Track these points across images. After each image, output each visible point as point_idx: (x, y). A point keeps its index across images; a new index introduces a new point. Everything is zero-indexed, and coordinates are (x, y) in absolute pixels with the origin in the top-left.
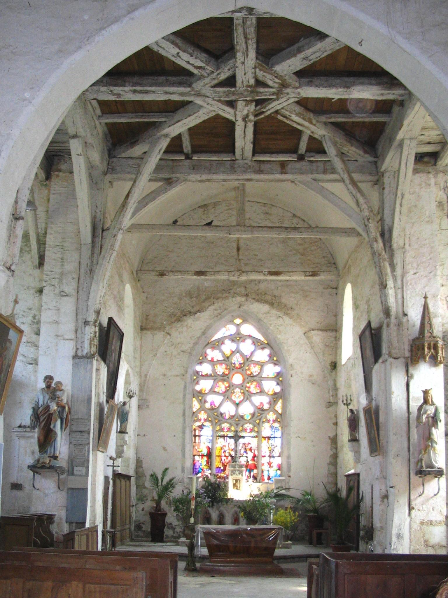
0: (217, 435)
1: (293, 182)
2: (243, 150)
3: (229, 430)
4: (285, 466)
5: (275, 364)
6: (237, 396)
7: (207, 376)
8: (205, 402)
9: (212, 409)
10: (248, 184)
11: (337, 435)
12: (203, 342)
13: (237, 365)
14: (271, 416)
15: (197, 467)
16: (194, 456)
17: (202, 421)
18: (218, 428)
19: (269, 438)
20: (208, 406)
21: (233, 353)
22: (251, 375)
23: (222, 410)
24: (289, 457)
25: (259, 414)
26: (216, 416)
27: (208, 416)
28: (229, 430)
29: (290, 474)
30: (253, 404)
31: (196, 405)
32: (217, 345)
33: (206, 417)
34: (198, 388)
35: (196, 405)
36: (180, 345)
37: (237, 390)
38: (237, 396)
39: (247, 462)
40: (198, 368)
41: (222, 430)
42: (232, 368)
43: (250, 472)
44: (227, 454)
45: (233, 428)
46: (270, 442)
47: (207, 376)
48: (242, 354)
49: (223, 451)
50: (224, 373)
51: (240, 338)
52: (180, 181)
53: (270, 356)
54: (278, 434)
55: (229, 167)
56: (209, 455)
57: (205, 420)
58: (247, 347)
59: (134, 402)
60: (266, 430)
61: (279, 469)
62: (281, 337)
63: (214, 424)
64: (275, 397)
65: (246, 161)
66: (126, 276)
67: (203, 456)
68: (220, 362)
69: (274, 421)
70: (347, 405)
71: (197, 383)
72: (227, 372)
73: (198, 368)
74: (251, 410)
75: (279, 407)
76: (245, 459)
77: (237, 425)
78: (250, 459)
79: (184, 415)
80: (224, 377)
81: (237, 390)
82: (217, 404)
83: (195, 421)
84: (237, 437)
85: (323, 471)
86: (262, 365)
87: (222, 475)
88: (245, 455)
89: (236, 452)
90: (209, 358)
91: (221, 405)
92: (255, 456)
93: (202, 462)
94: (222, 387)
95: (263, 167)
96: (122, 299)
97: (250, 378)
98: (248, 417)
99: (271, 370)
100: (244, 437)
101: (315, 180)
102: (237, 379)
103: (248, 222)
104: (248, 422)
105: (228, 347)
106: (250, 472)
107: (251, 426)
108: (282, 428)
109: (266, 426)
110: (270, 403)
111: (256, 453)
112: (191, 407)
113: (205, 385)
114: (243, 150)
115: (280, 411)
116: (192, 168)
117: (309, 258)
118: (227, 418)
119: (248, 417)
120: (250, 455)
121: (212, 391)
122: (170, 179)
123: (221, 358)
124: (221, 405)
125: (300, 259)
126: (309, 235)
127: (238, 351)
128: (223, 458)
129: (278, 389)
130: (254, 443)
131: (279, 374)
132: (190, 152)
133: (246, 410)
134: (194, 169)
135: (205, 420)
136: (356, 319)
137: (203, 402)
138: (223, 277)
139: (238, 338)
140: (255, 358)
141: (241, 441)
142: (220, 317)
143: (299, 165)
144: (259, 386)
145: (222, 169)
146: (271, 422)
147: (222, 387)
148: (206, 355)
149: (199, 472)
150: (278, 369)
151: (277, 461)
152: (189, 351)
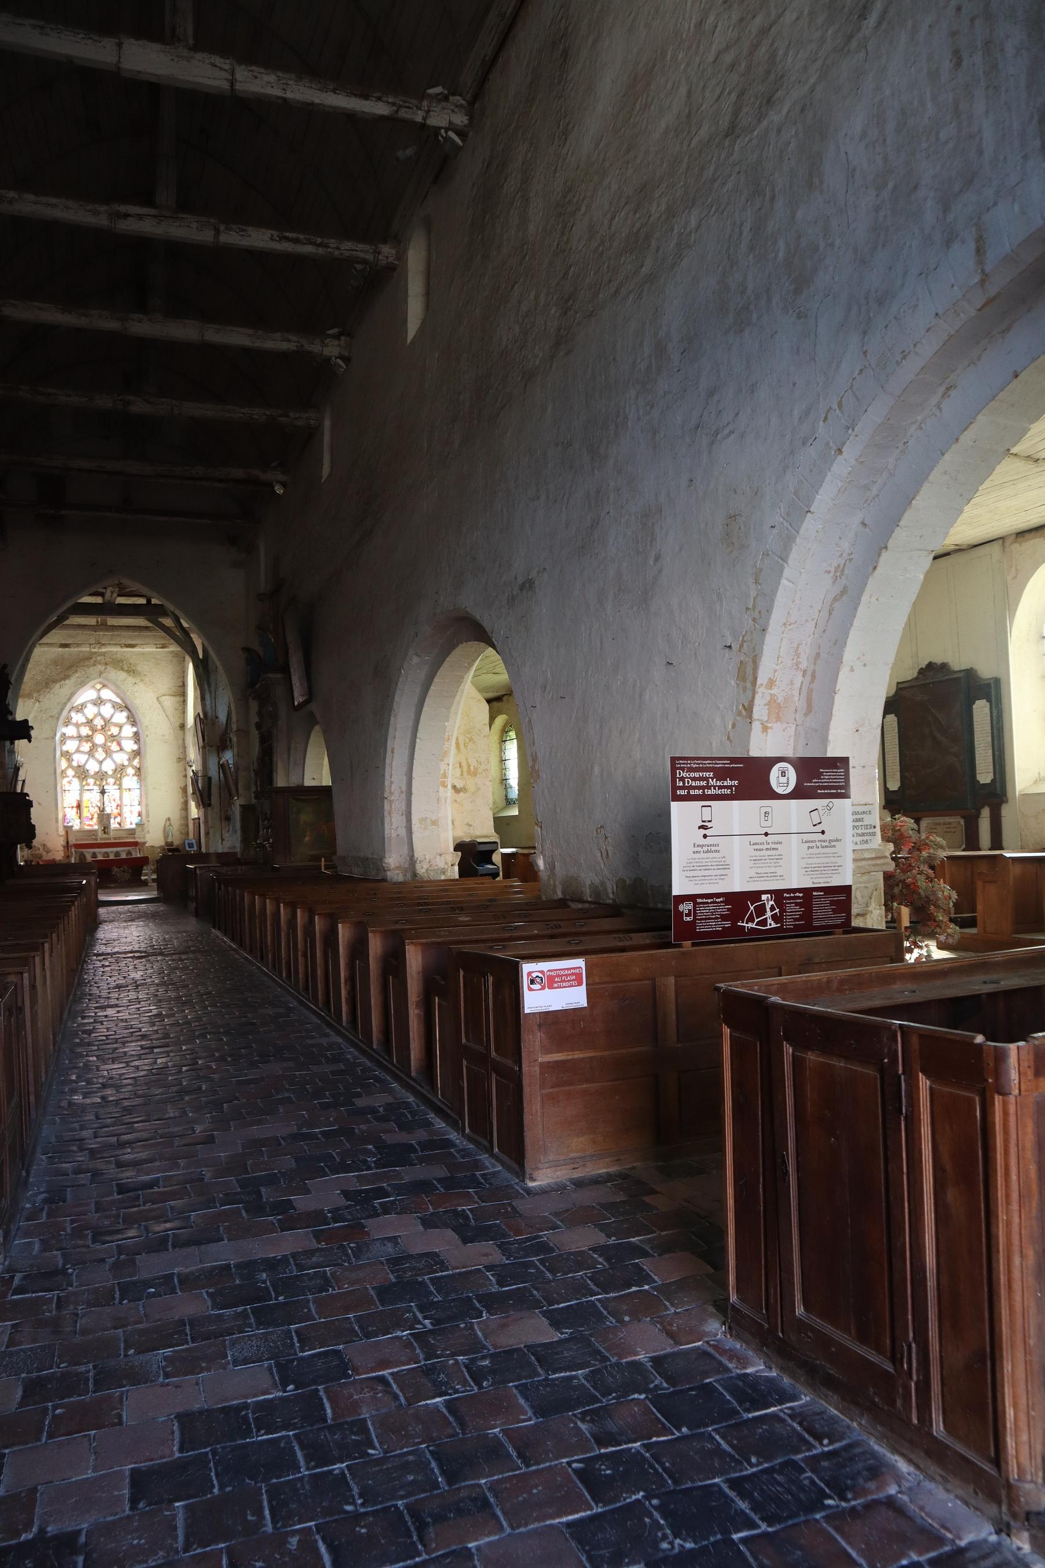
4: (144, 813)
6: (100, 754)
12: (68, 708)
14: (131, 771)
20: (75, 764)
21: (95, 716)
22: (112, 736)
23: (87, 767)
24: (147, 806)
25: (120, 770)
26: (82, 773)
30: (114, 761)
31: (64, 764)
32: (80, 709)
34: (65, 748)
35: (64, 764)
37: (100, 750)
38: (100, 754)
40: (64, 730)
41: (88, 784)
47: (72, 737)
48: (103, 718)
62: (137, 702)
72: (90, 733)
75: (136, 763)
80: (89, 738)
81: (100, 750)
87: (91, 823)
90: (74, 721)
94: (86, 747)
98: (110, 773)
105: (91, 711)
113: (71, 746)
119: (110, 773)
120: (114, 805)
121: (78, 751)
129: (135, 747)
133: (108, 767)
138: (85, 649)
139: (99, 702)
140: (114, 720)
144: (119, 744)
147: (86, 747)
150: (135, 729)
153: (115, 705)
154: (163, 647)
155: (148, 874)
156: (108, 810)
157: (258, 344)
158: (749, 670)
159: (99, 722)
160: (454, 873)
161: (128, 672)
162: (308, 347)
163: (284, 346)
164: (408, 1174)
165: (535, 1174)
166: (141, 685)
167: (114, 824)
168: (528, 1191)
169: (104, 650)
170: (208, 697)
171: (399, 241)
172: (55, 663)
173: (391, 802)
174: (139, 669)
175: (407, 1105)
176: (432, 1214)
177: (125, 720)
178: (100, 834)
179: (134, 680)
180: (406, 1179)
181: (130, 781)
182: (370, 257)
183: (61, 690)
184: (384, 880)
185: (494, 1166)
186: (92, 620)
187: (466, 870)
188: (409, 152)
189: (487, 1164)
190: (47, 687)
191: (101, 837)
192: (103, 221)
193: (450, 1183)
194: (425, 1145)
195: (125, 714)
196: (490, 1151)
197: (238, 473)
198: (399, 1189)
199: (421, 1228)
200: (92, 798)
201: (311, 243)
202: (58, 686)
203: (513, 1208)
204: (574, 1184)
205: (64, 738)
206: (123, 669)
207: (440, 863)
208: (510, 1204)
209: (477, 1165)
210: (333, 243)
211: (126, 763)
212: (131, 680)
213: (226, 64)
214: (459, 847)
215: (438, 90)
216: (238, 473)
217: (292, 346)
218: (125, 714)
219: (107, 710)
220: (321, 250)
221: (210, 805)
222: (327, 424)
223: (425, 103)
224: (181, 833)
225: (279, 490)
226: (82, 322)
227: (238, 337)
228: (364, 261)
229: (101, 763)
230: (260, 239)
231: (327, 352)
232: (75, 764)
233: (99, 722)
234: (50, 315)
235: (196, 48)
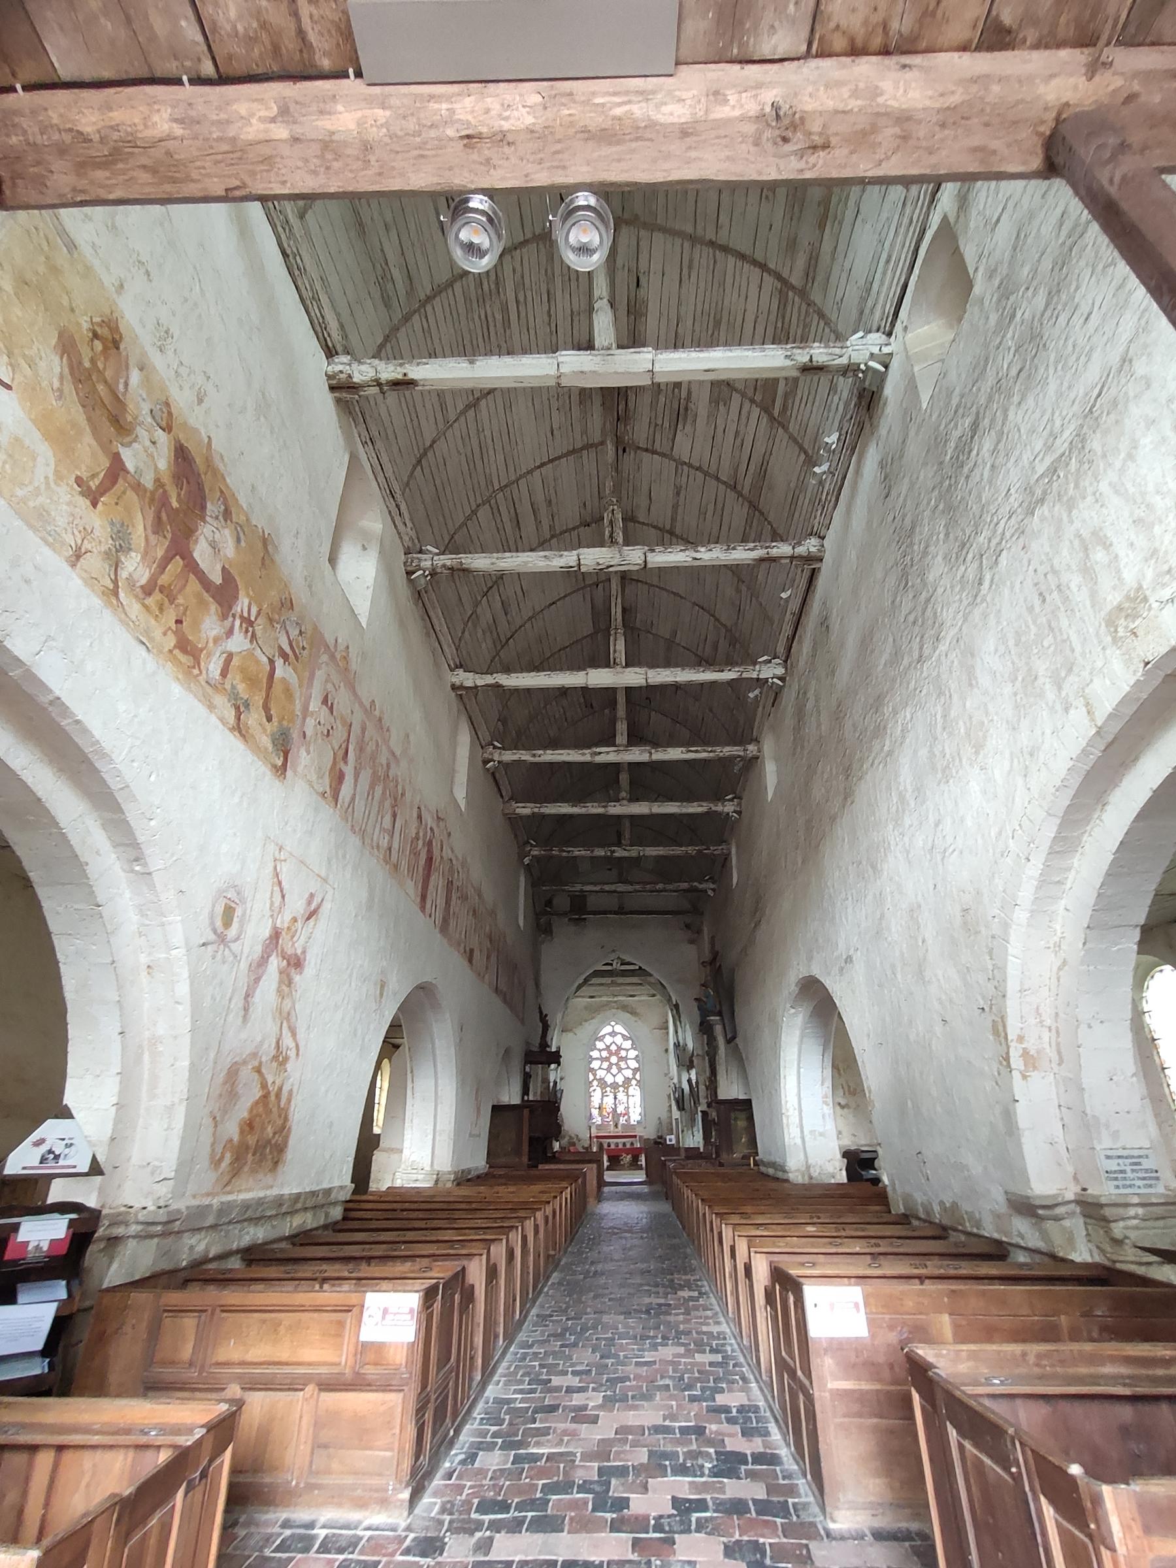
6: (614, 1070)
14: (634, 1082)
25: (627, 1081)
26: (603, 1083)
32: (601, 1039)
35: (591, 1077)
38: (614, 1070)
42: (611, 1054)
60: (631, 1091)
64: (635, 1070)
75: (638, 1077)
86: (627, 1050)
93: (595, 1112)
94: (605, 1065)
99: (633, 1054)
102: (614, 1059)
105: (608, 1040)
133: (620, 1079)
137: (595, 1075)
147: (605, 1065)
150: (636, 1053)
151: (639, 1110)
153: (623, 1035)
157: (684, 811)
158: (1001, 1028)
159: (614, 1048)
160: (843, 1177)
162: (714, 808)
163: (700, 810)
164: (734, 1489)
165: (836, 1514)
167: (622, 1121)
168: (828, 1534)
171: (757, 741)
173: (788, 1117)
175: (756, 1409)
176: (737, 1541)
180: (729, 1495)
181: (635, 1091)
182: (742, 753)
183: (589, 1027)
184: (787, 1181)
185: (806, 1495)
186: (608, 980)
187: (852, 1174)
188: (757, 692)
189: (802, 1491)
191: (612, 1131)
192: (588, 758)
193: (764, 1507)
194: (759, 1458)
196: (805, 1476)
197: (685, 885)
198: (720, 1506)
199: (722, 1557)
200: (609, 1101)
201: (705, 751)
203: (808, 1551)
204: (873, 1535)
205: (592, 1059)
207: (830, 1169)
208: (807, 1546)
209: (792, 1490)
210: (718, 749)
212: (634, 1019)
213: (642, 670)
214: (846, 1154)
215: (765, 658)
216: (685, 885)
217: (704, 809)
219: (619, 1039)
220: (711, 755)
222: (734, 851)
223: (757, 667)
225: (710, 893)
226: (583, 811)
227: (672, 808)
228: (739, 756)
230: (675, 754)
231: (726, 810)
233: (614, 1048)
234: (565, 809)
235: (627, 666)
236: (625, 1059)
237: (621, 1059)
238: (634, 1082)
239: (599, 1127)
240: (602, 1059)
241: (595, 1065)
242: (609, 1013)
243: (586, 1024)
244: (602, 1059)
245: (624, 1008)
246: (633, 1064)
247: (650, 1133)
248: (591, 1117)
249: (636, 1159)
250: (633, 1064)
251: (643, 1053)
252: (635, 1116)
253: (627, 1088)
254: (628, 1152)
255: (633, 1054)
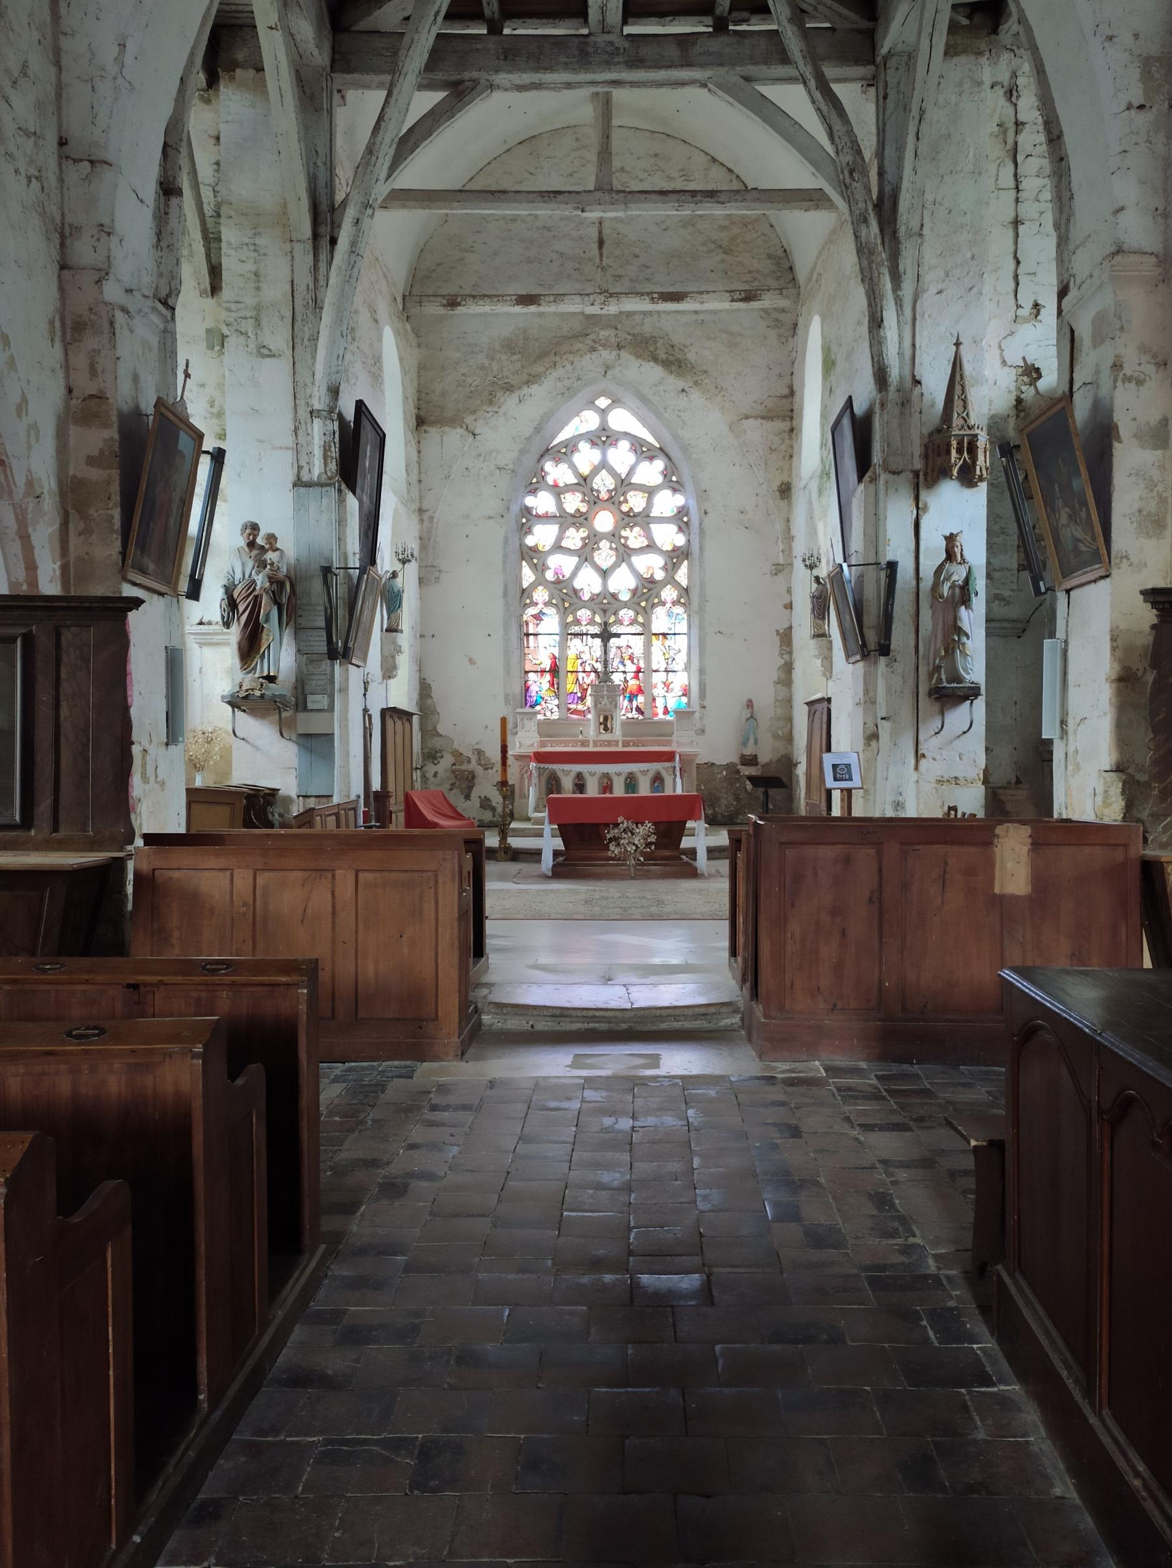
0: (567, 633)
1: (704, 85)
2: (603, 9)
3: (592, 622)
5: (675, 490)
6: (605, 555)
7: (546, 518)
8: (545, 568)
9: (558, 582)
10: (618, 94)
11: (791, 628)
13: (604, 495)
14: (669, 594)
15: (533, 694)
16: (527, 672)
17: (540, 606)
18: (570, 619)
19: (665, 635)
20: (550, 576)
23: (577, 584)
24: (702, 671)
26: (565, 596)
27: (552, 597)
28: (592, 622)
29: (705, 703)
31: (528, 576)
33: (547, 598)
35: (528, 576)
36: (494, 455)
37: (604, 544)
38: (605, 555)
39: (626, 681)
40: (530, 501)
41: (577, 622)
43: (631, 701)
44: (588, 669)
45: (598, 619)
46: (667, 643)
47: (546, 518)
48: (613, 472)
49: (580, 661)
50: (578, 510)
51: (608, 437)
52: (479, 88)
53: (666, 474)
54: (682, 627)
55: (576, 53)
56: (554, 670)
57: (546, 604)
58: (621, 457)
59: (412, 569)
60: (660, 620)
61: (684, 695)
63: (564, 612)
64: (675, 557)
65: (609, 38)
66: (384, 308)
67: (543, 672)
68: (569, 488)
69: (674, 603)
70: (811, 567)
71: (529, 531)
72: (584, 508)
73: (530, 501)
74: (632, 583)
75: (682, 576)
76: (622, 676)
77: (605, 611)
78: (629, 676)
79: (505, 595)
80: (580, 519)
82: (567, 574)
83: (526, 606)
84: (606, 636)
85: (766, 696)
86: (650, 492)
87: (580, 707)
88: (622, 668)
89: (606, 663)
91: (575, 573)
92: (638, 671)
93: (540, 685)
94: (574, 538)
95: (645, 51)
96: (377, 361)
97: (627, 519)
98: (625, 597)
99: (667, 503)
100: (618, 635)
101: (748, 79)
102: (604, 521)
103: (617, 185)
104: (625, 605)
105: (586, 458)
106: (631, 701)
107: (631, 613)
108: (689, 616)
109: (660, 612)
110: (665, 568)
111: (642, 665)
112: (519, 578)
114: (603, 9)
115: (684, 583)
116: (502, 57)
117: (739, 259)
118: (586, 597)
119: (625, 597)
120: (631, 668)
121: (558, 548)
122: (460, 83)
123: (572, 480)
124: (575, 573)
125: (722, 261)
126: (737, 208)
127: (604, 465)
128: (581, 675)
129: (680, 540)
130: (637, 644)
131: (682, 511)
132: (496, 16)
133: (622, 583)
134: (506, 59)
135: (546, 604)
136: (829, 391)
137: (540, 569)
141: (614, 642)
142: (573, 396)
143: (715, 45)
145: (562, 59)
146: (668, 605)
147: (574, 538)
148: (542, 475)
149: (536, 704)
150: (680, 500)
151: (680, 680)
152: (511, 467)
154: (749, 297)
155: (700, 838)
156: (617, 678)
159: (604, 483)
161: (666, 364)
166: (696, 395)
167: (624, 711)
169: (612, 309)
170: (890, 315)
172: (510, 346)
174: (691, 356)
177: (659, 479)
178: (591, 731)
179: (680, 383)
190: (491, 403)
191: (591, 736)
195: (659, 464)
202: (515, 396)
206: (655, 359)
211: (659, 575)
212: (674, 382)
218: (659, 464)
219: (621, 457)
221: (884, 650)
224: (776, 736)
229: (605, 574)
232: (550, 576)
233: (604, 483)
236: (643, 519)
237: (629, 519)
238: (669, 594)
239: (547, 728)
240: (565, 520)
241: (542, 536)
242: (589, 364)
243: (510, 402)
244: (565, 520)
245: (646, 346)
246: (668, 536)
247: (717, 746)
248: (525, 697)
249: (669, 833)
250: (668, 536)
251: (703, 495)
252: (670, 693)
253: (647, 612)
254: (636, 809)
255: (667, 503)
